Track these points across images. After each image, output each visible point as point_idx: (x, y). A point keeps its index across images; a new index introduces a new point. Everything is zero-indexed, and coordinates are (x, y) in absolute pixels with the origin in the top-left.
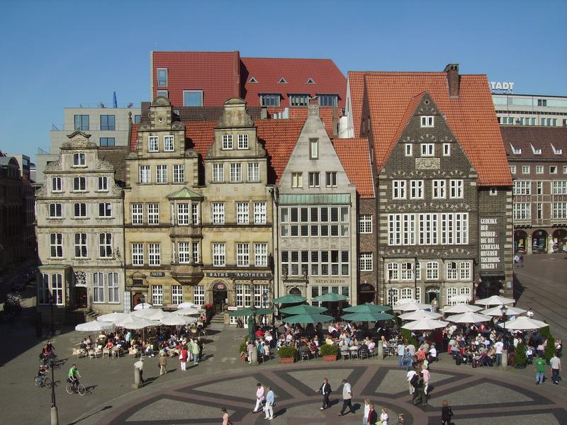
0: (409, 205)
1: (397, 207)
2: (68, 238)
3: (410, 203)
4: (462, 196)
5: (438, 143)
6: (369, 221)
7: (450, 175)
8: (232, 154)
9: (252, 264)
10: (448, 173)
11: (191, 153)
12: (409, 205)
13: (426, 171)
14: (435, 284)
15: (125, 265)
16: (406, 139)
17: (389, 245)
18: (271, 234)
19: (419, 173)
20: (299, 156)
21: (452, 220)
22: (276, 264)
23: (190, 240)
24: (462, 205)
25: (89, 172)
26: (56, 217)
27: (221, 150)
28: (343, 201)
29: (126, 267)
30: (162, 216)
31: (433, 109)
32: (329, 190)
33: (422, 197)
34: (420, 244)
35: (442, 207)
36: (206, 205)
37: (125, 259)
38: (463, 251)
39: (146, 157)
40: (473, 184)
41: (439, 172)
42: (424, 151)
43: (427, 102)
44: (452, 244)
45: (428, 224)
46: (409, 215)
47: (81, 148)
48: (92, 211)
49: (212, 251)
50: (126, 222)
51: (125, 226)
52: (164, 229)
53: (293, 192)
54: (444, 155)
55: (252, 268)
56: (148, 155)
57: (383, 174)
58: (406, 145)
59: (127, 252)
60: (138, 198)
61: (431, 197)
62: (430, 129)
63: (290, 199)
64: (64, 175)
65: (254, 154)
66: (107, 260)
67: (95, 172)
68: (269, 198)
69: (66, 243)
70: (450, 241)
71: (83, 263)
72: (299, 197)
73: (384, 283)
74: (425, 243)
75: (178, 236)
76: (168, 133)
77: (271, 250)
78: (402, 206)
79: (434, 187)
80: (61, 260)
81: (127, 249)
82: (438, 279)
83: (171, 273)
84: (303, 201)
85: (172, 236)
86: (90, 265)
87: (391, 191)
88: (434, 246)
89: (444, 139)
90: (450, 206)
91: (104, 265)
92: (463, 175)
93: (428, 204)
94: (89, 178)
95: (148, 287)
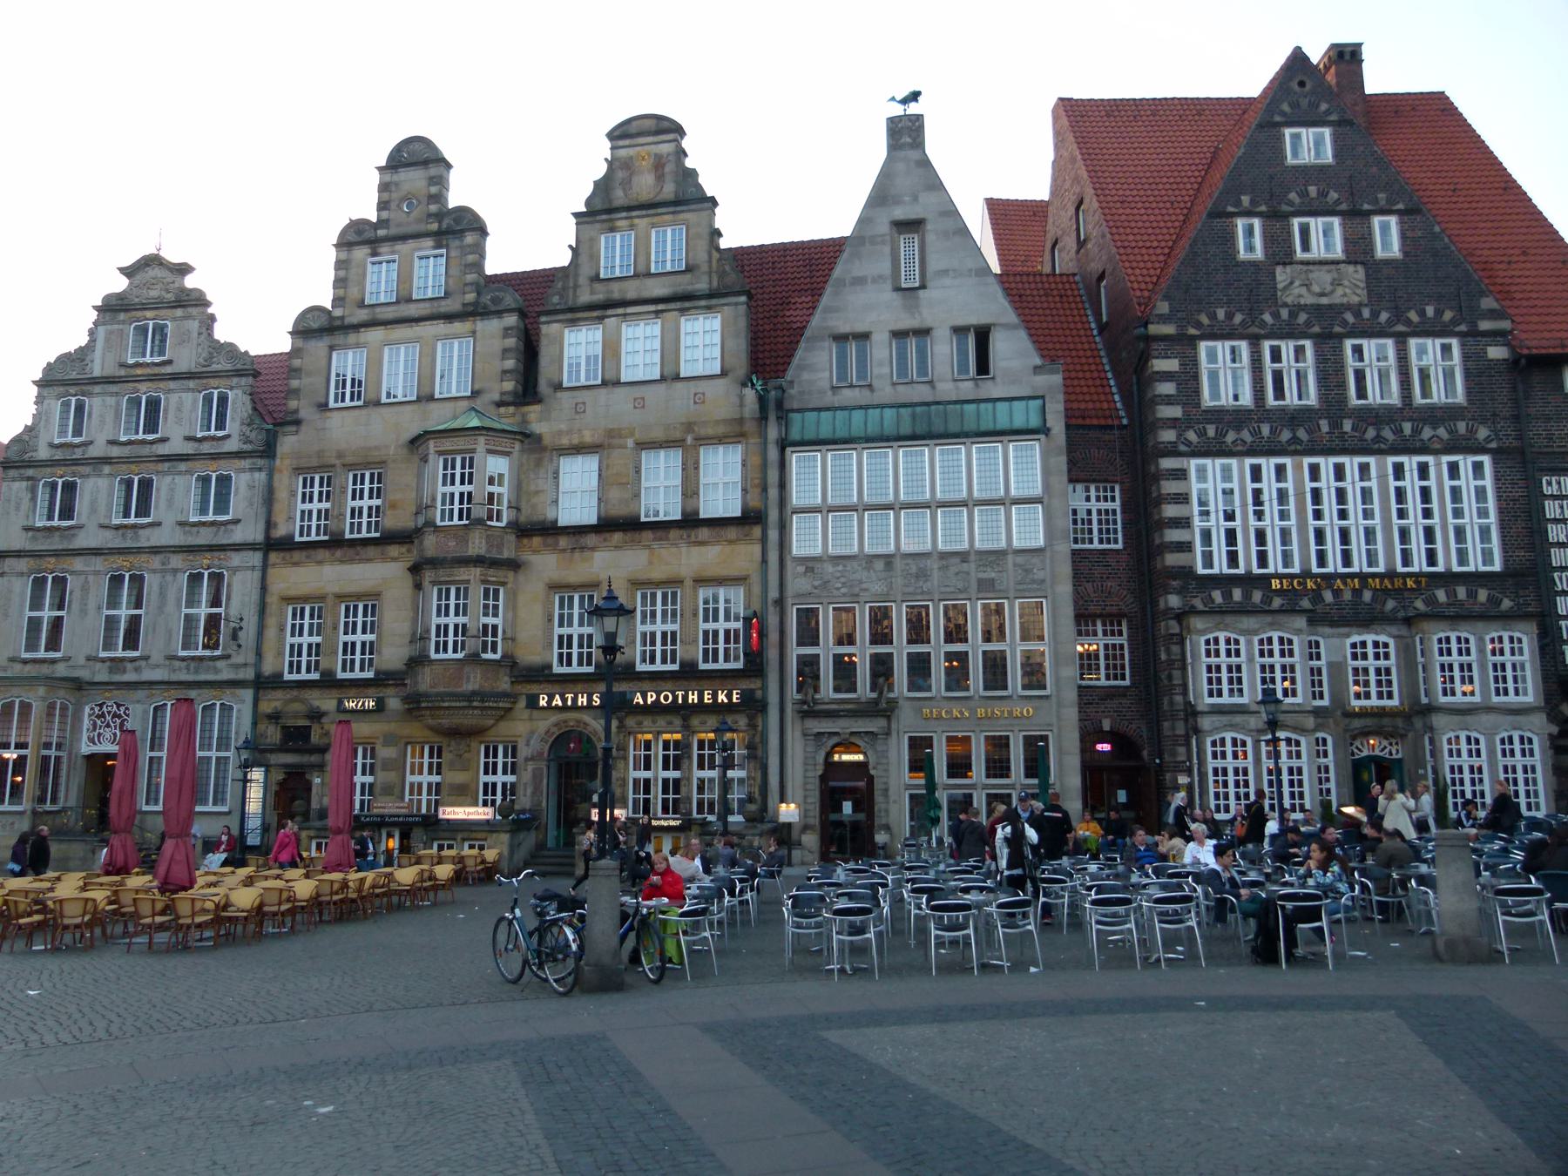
0: (1266, 430)
1: (1221, 434)
2: (85, 589)
3: (1269, 420)
4: (1460, 397)
5: (1355, 216)
6: (1109, 505)
7: (1409, 322)
8: (632, 290)
9: (688, 657)
10: (1398, 316)
11: (495, 301)
12: (1266, 430)
13: (1317, 311)
14: (1386, 721)
15: (258, 675)
16: (1238, 203)
17: (1201, 570)
18: (757, 549)
19: (1293, 315)
20: (860, 281)
21: (1432, 483)
22: (772, 654)
23: (474, 574)
24: (1462, 427)
25: (175, 377)
26: (56, 522)
27: (596, 278)
28: (1019, 423)
29: (264, 683)
30: (393, 506)
31: (1324, 107)
32: (967, 389)
33: (1312, 399)
34: (1315, 570)
35: (1387, 434)
36: (538, 463)
37: (259, 654)
38: (1483, 595)
39: (354, 320)
40: (1496, 352)
41: (1366, 313)
42: (1306, 246)
43: (1302, 84)
44: (1440, 568)
45: (1341, 495)
46: (1268, 465)
47: (158, 305)
48: (170, 501)
49: (550, 620)
50: (280, 531)
51: (275, 546)
52: (394, 550)
53: (830, 399)
54: (1380, 253)
55: (689, 673)
56: (362, 315)
57: (1163, 319)
58: (1240, 223)
59: (271, 633)
60: (320, 454)
61: (1343, 399)
62: (1322, 169)
63: (826, 425)
64: (97, 389)
65: (702, 286)
66: (201, 659)
67: (190, 376)
68: (750, 427)
69: (75, 606)
70: (1431, 558)
71: (124, 671)
72: (858, 416)
73: (1191, 713)
74: (1334, 564)
75: (434, 563)
76: (429, 242)
77: (756, 606)
78: (1238, 429)
79: (1350, 362)
80: (53, 661)
81: (271, 622)
82: (1395, 702)
83: (406, 699)
84: (872, 429)
85: (415, 569)
86: (149, 675)
87: (1196, 377)
88: (1374, 575)
89: (1376, 201)
90: (1416, 431)
91: (190, 678)
92: (1454, 322)
93: (1336, 425)
94: (174, 398)
95: (323, 750)
